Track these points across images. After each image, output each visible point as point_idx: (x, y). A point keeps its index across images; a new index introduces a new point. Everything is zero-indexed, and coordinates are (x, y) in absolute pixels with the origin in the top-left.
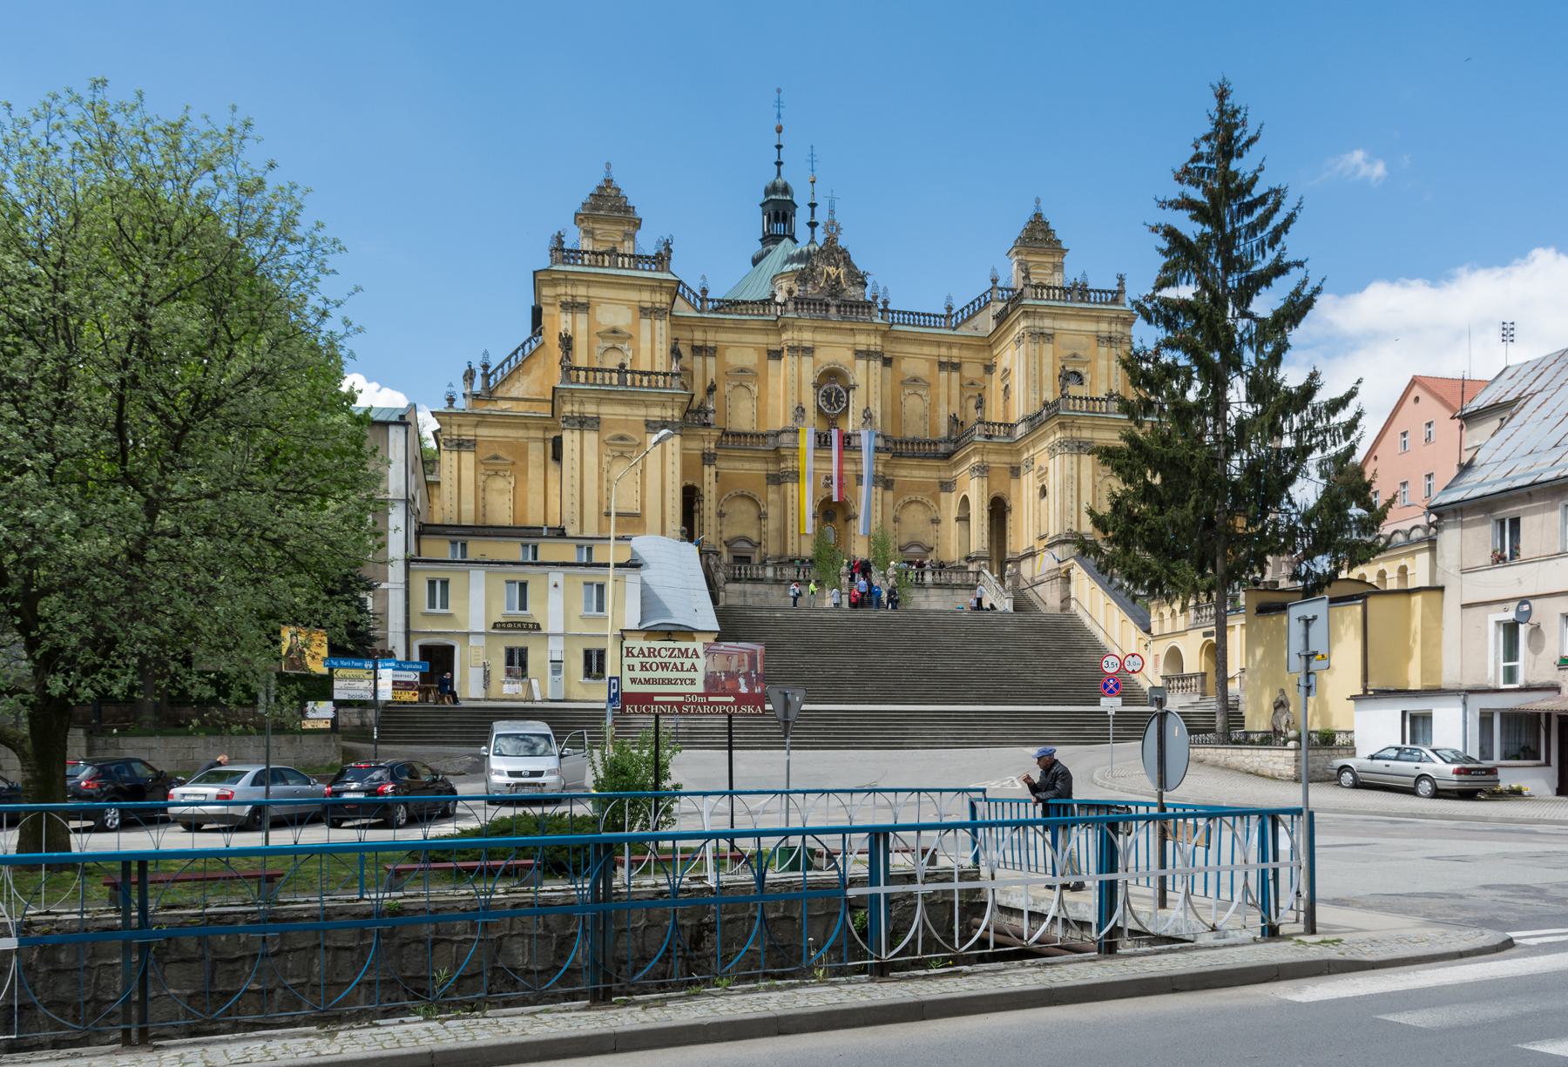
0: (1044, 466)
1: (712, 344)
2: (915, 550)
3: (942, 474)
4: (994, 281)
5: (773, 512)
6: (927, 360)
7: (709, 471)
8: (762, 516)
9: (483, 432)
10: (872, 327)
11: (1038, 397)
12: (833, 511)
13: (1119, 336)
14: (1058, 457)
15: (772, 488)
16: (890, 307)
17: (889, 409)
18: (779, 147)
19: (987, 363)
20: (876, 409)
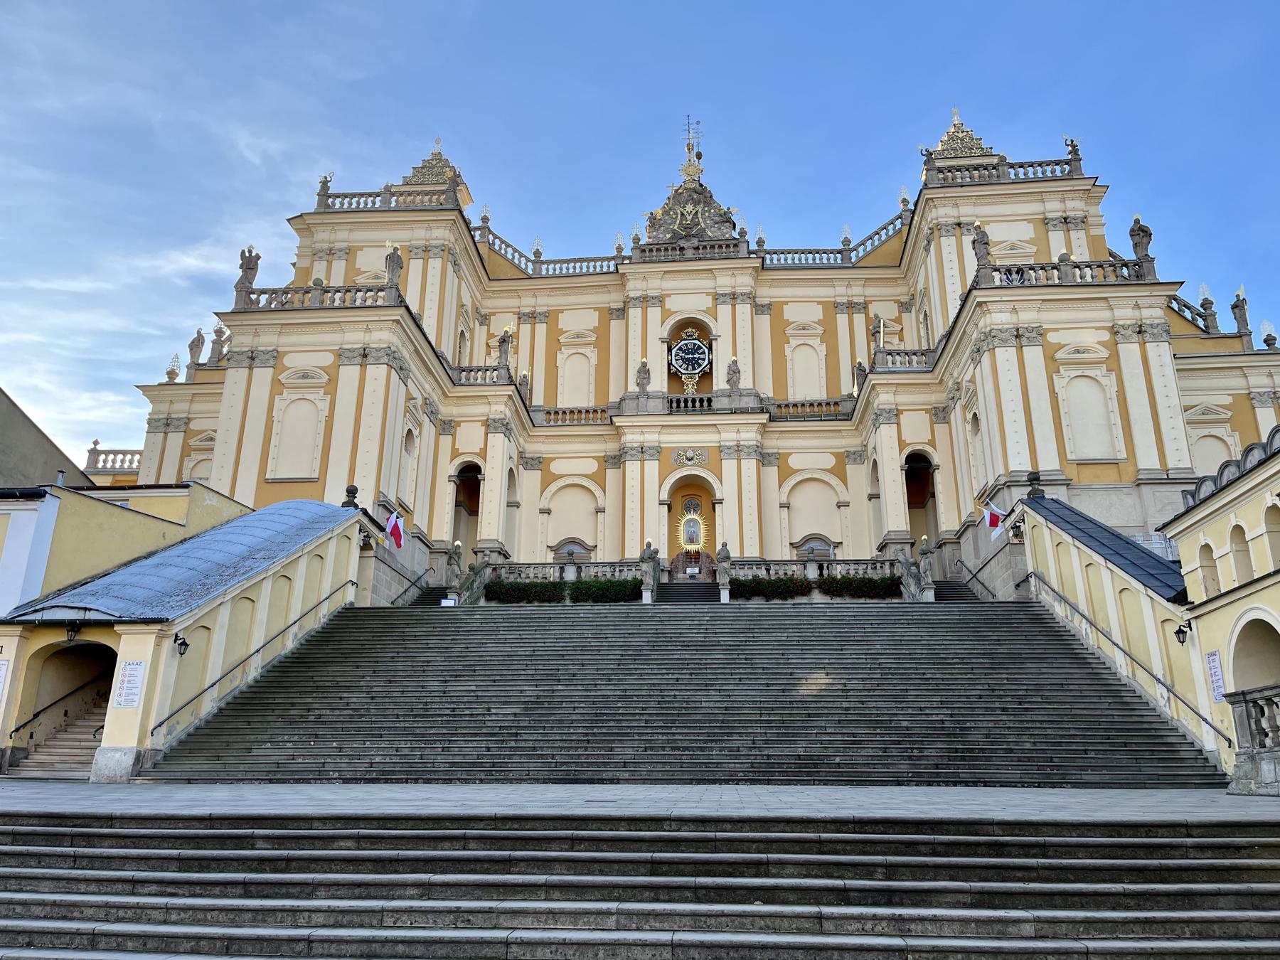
13: (1080, 214)
14: (986, 358)
19: (904, 299)
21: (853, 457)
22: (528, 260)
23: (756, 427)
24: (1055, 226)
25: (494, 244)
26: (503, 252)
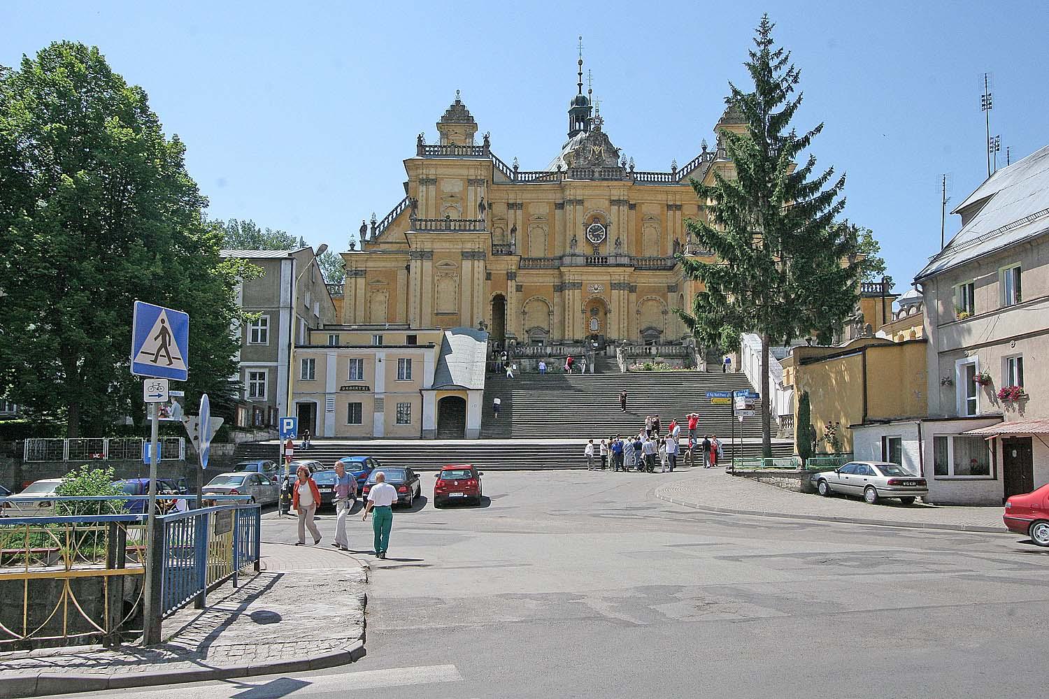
2: (650, 332)
5: (557, 310)
7: (511, 285)
9: (370, 264)
12: (597, 307)
15: (557, 294)
18: (580, 74)
20: (624, 238)
22: (511, 171)
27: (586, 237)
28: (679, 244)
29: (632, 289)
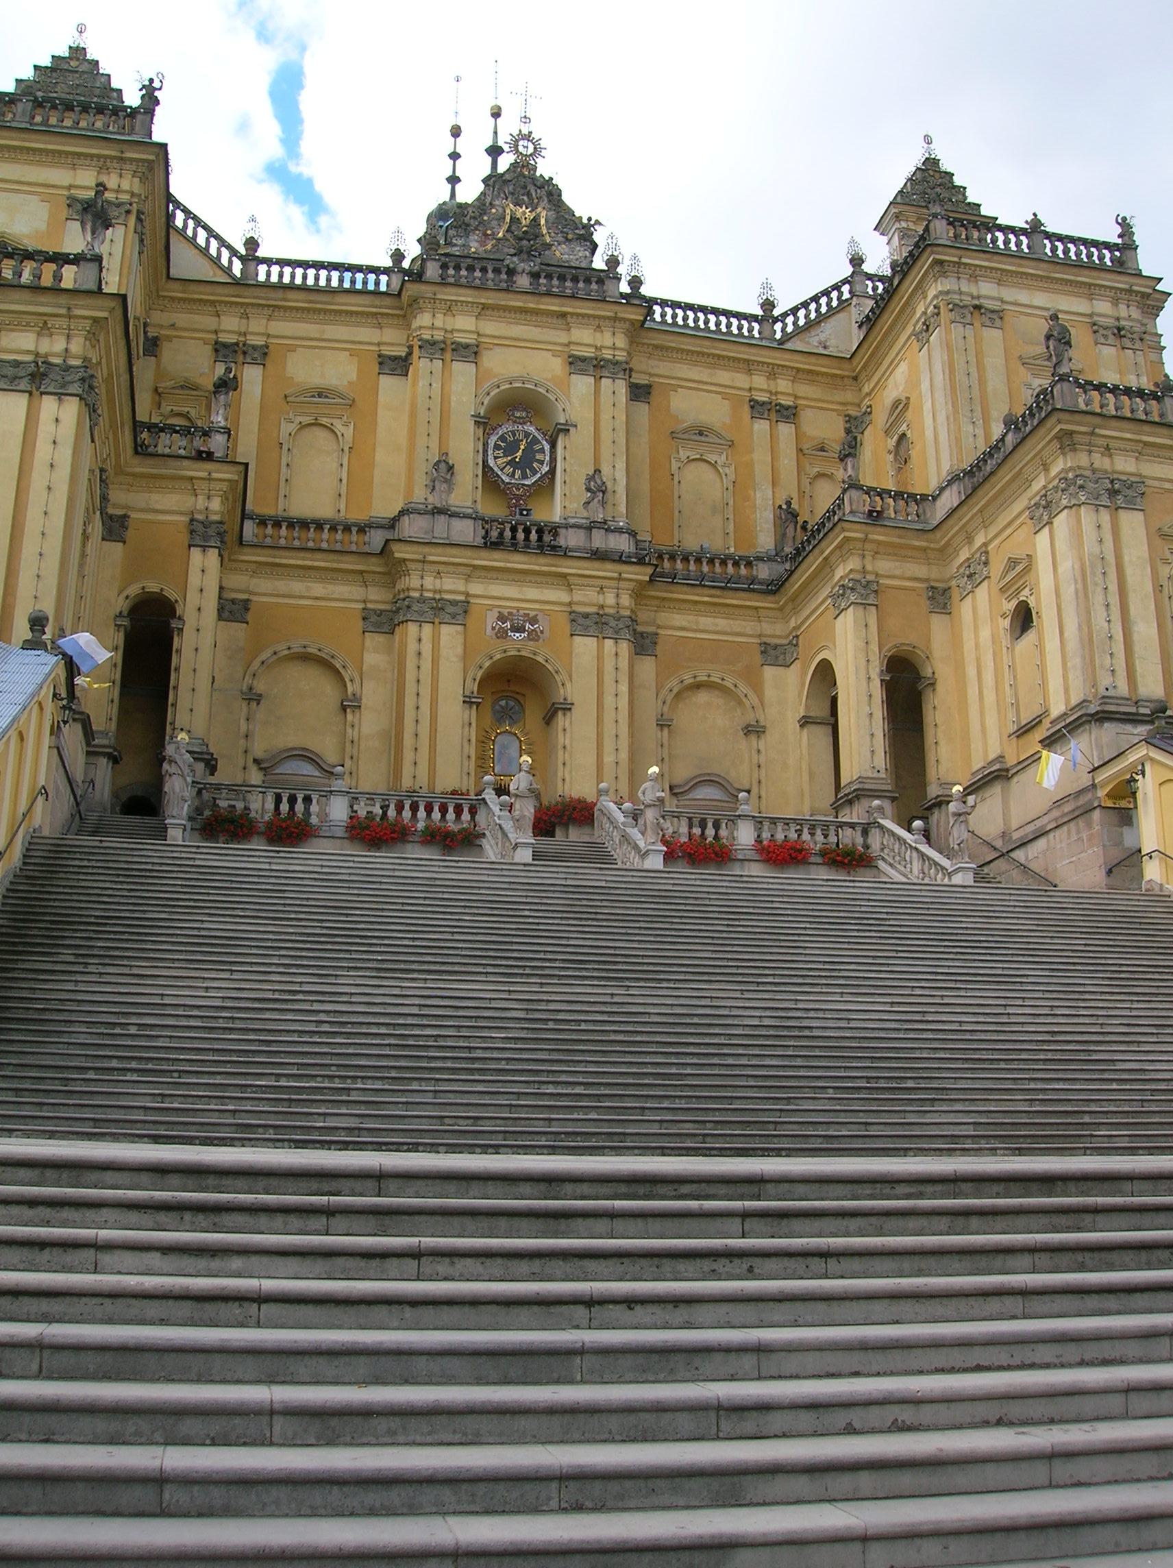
0: (1019, 553)
1: (259, 341)
3: (767, 628)
4: (857, 261)
5: (373, 695)
6: (726, 396)
8: (348, 705)
10: (607, 311)
11: (980, 432)
14: (1062, 521)
15: (373, 640)
16: (645, 290)
17: (645, 487)
18: (455, 156)
20: (616, 475)
21: (772, 652)
22: (234, 252)
23: (632, 585)
24: (1105, 336)
25: (174, 216)
26: (190, 232)
27: (485, 462)
28: (795, 516)
29: (643, 644)
